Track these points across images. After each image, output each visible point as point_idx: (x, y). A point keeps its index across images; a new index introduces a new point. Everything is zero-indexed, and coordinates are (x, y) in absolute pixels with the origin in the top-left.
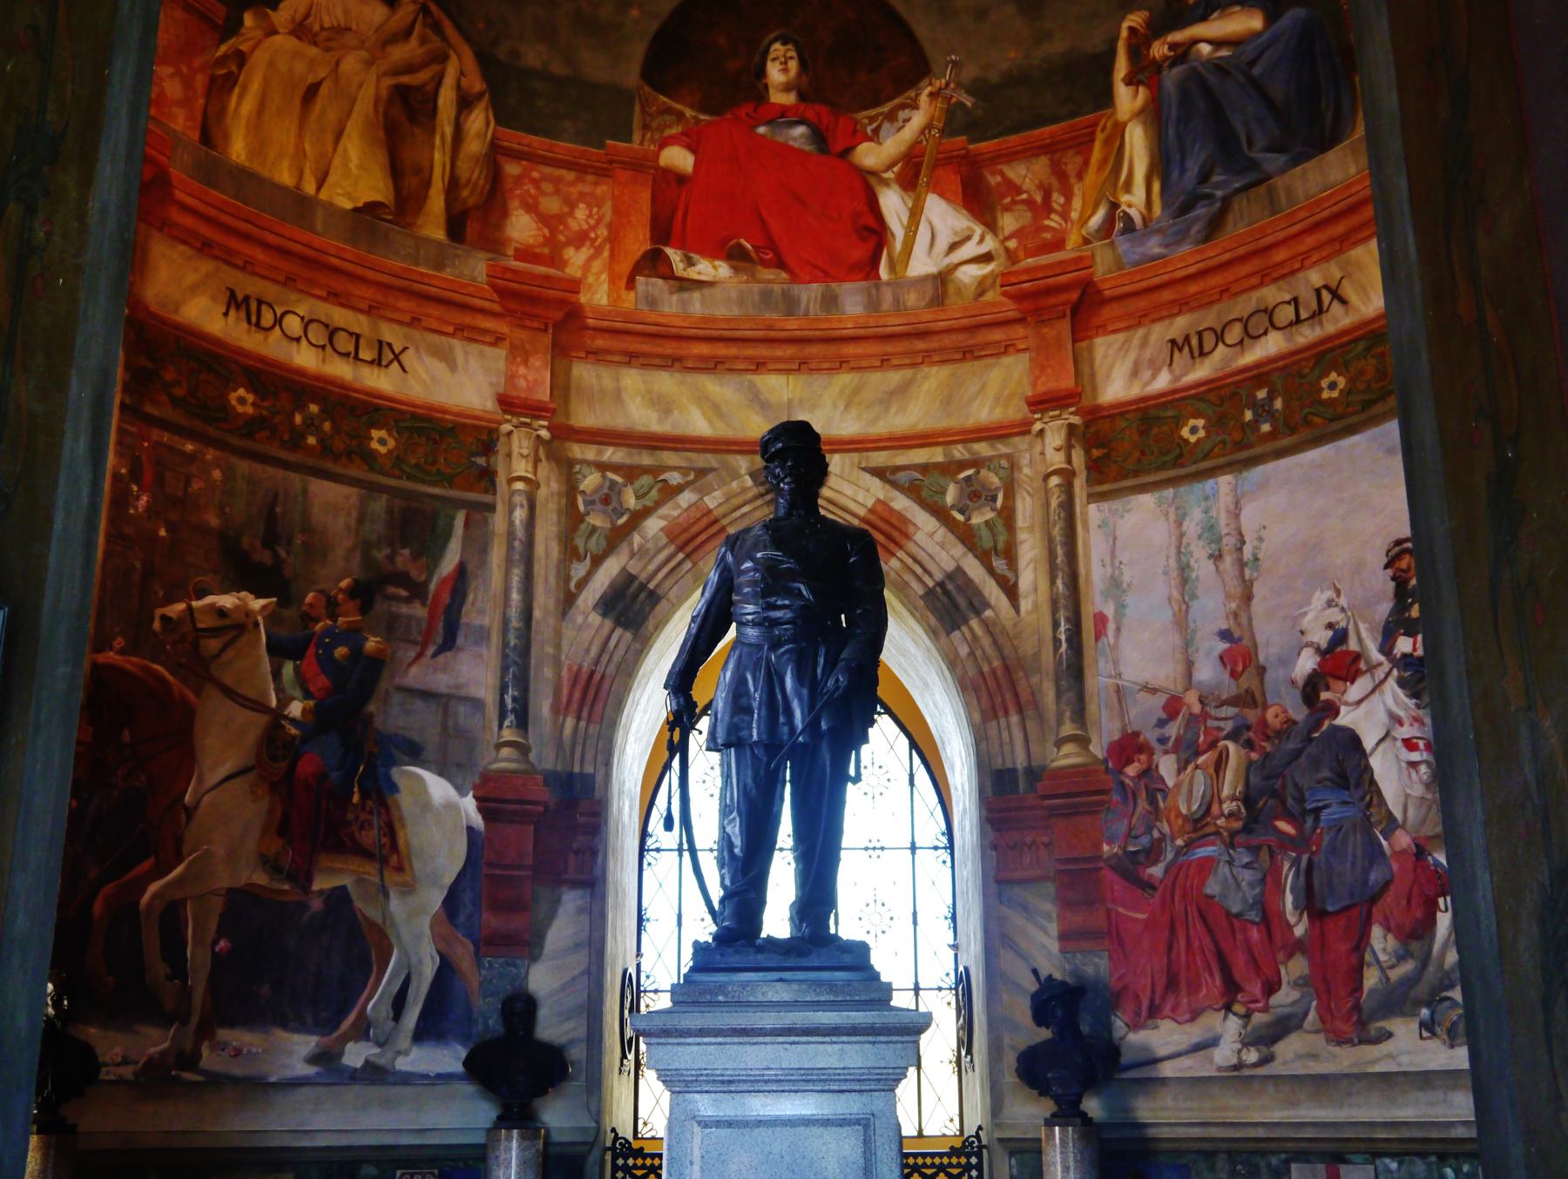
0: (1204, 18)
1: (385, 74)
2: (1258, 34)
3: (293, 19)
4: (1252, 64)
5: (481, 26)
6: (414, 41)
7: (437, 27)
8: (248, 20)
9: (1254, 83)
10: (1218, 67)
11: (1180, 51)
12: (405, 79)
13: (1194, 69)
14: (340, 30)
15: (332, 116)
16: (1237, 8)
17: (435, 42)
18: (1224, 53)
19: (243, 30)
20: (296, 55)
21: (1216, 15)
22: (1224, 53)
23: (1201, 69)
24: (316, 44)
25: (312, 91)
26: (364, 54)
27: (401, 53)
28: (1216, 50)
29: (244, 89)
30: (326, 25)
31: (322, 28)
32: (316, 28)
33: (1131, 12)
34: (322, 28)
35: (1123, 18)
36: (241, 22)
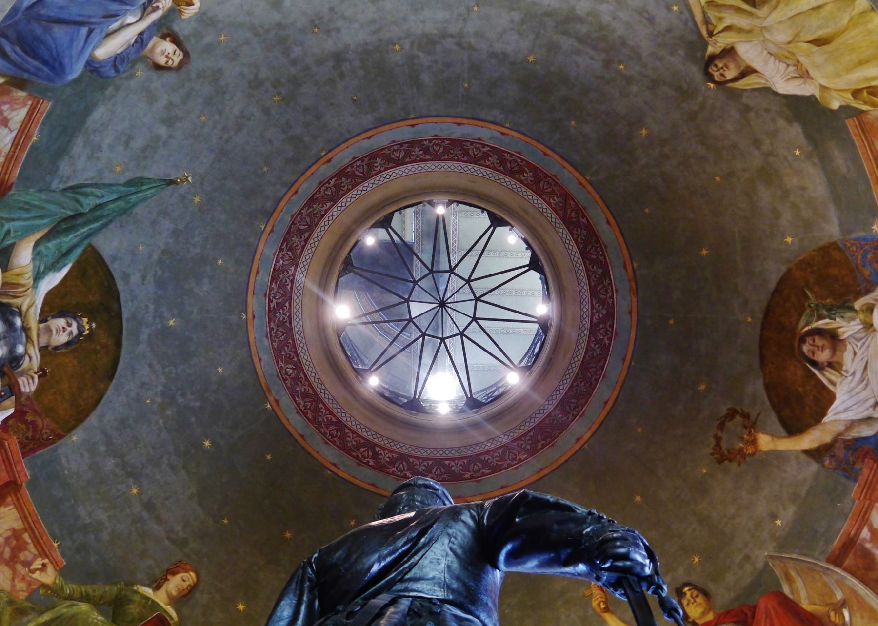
0: (141, 34)
1: (758, 17)
2: (95, 48)
3: (804, 83)
4: (90, 32)
5: (675, 8)
6: (727, 22)
7: (707, 21)
8: (835, 105)
9: (82, 24)
10: (114, 16)
11: (150, 9)
12: (745, 6)
13: (132, 6)
14: (777, 57)
15: (814, 21)
16: (119, 51)
17: (712, 14)
18: (115, 26)
19: (844, 104)
20: (817, 67)
21: (133, 41)
22: (115, 26)
23: (128, 8)
24: (798, 62)
25: (818, 42)
26: (767, 36)
27: (742, 21)
28: (122, 23)
29: (867, 79)
30: (785, 65)
31: (788, 65)
32: (791, 68)
33: (196, 14)
34: (788, 65)
35: (200, 8)
36: (841, 107)
